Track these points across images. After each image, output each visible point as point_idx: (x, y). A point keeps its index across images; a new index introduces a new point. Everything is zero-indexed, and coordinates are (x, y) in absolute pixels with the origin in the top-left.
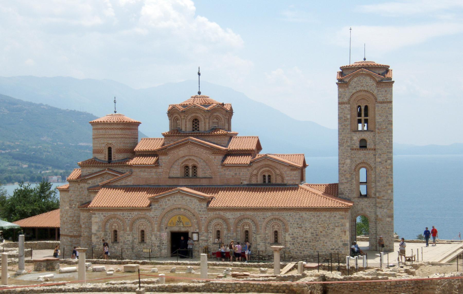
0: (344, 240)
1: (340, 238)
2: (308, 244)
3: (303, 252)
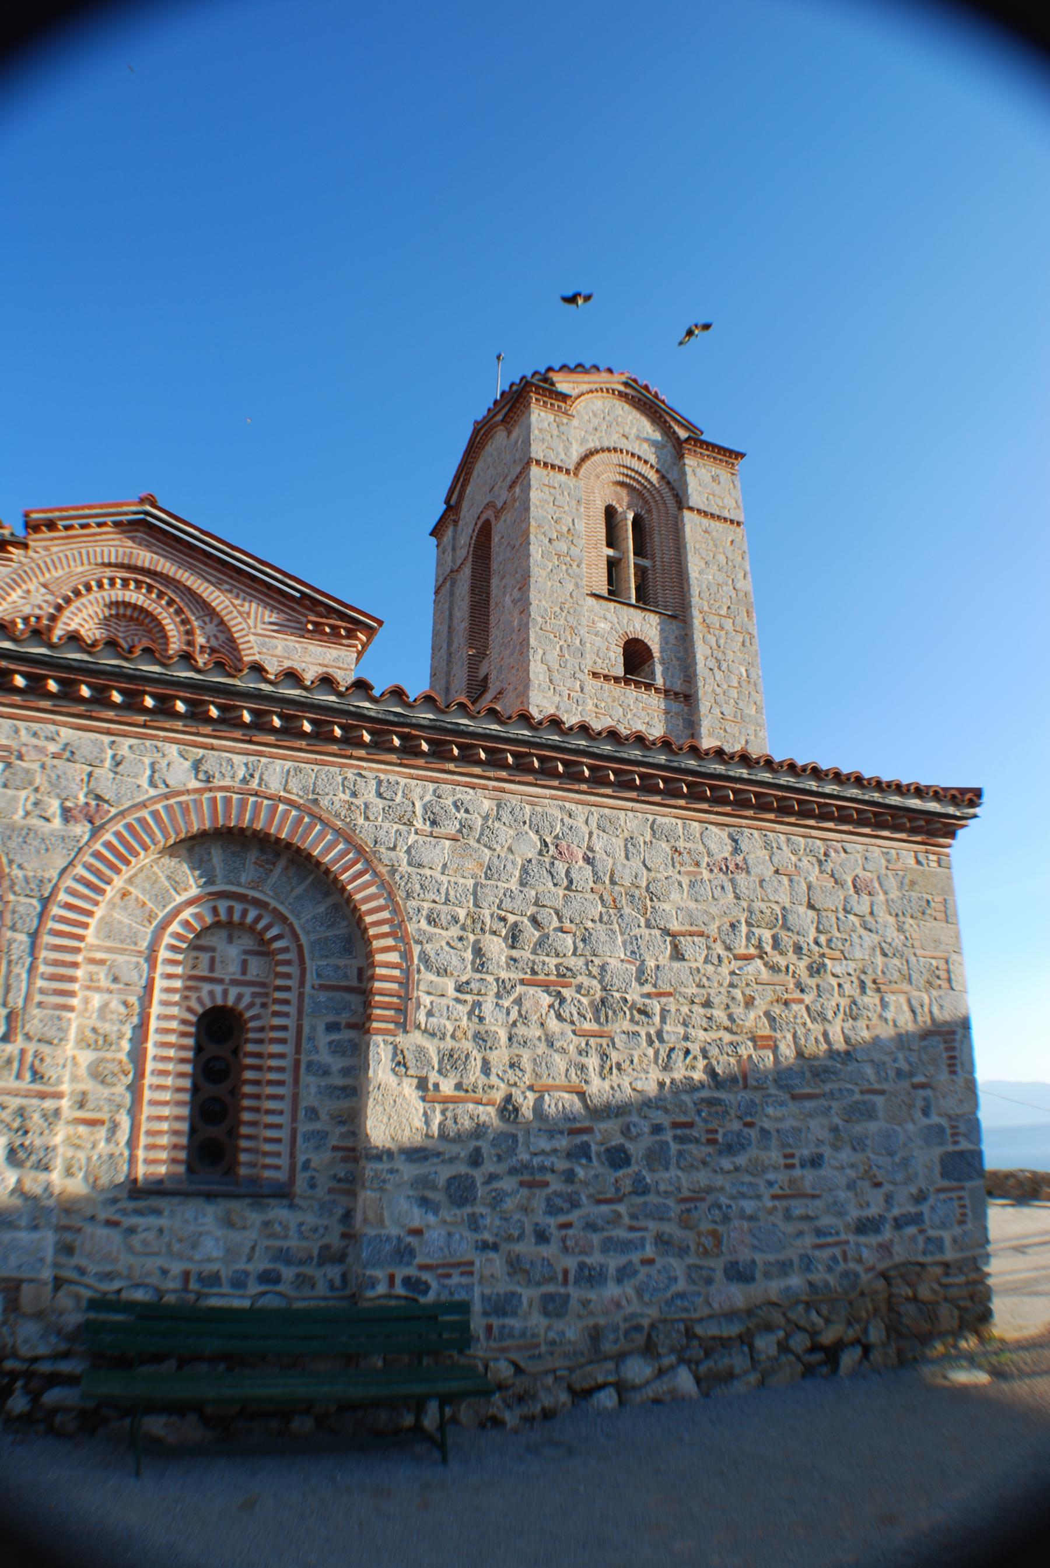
0: (944, 1122)
1: (920, 1103)
2: (641, 1188)
3: (575, 1293)
